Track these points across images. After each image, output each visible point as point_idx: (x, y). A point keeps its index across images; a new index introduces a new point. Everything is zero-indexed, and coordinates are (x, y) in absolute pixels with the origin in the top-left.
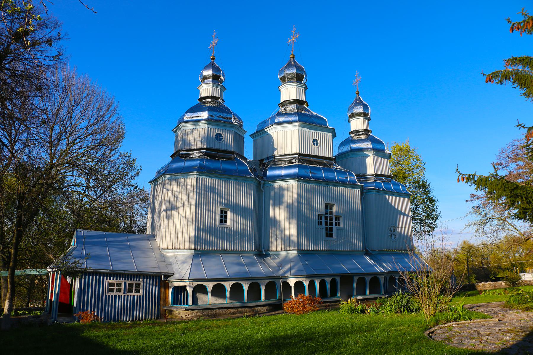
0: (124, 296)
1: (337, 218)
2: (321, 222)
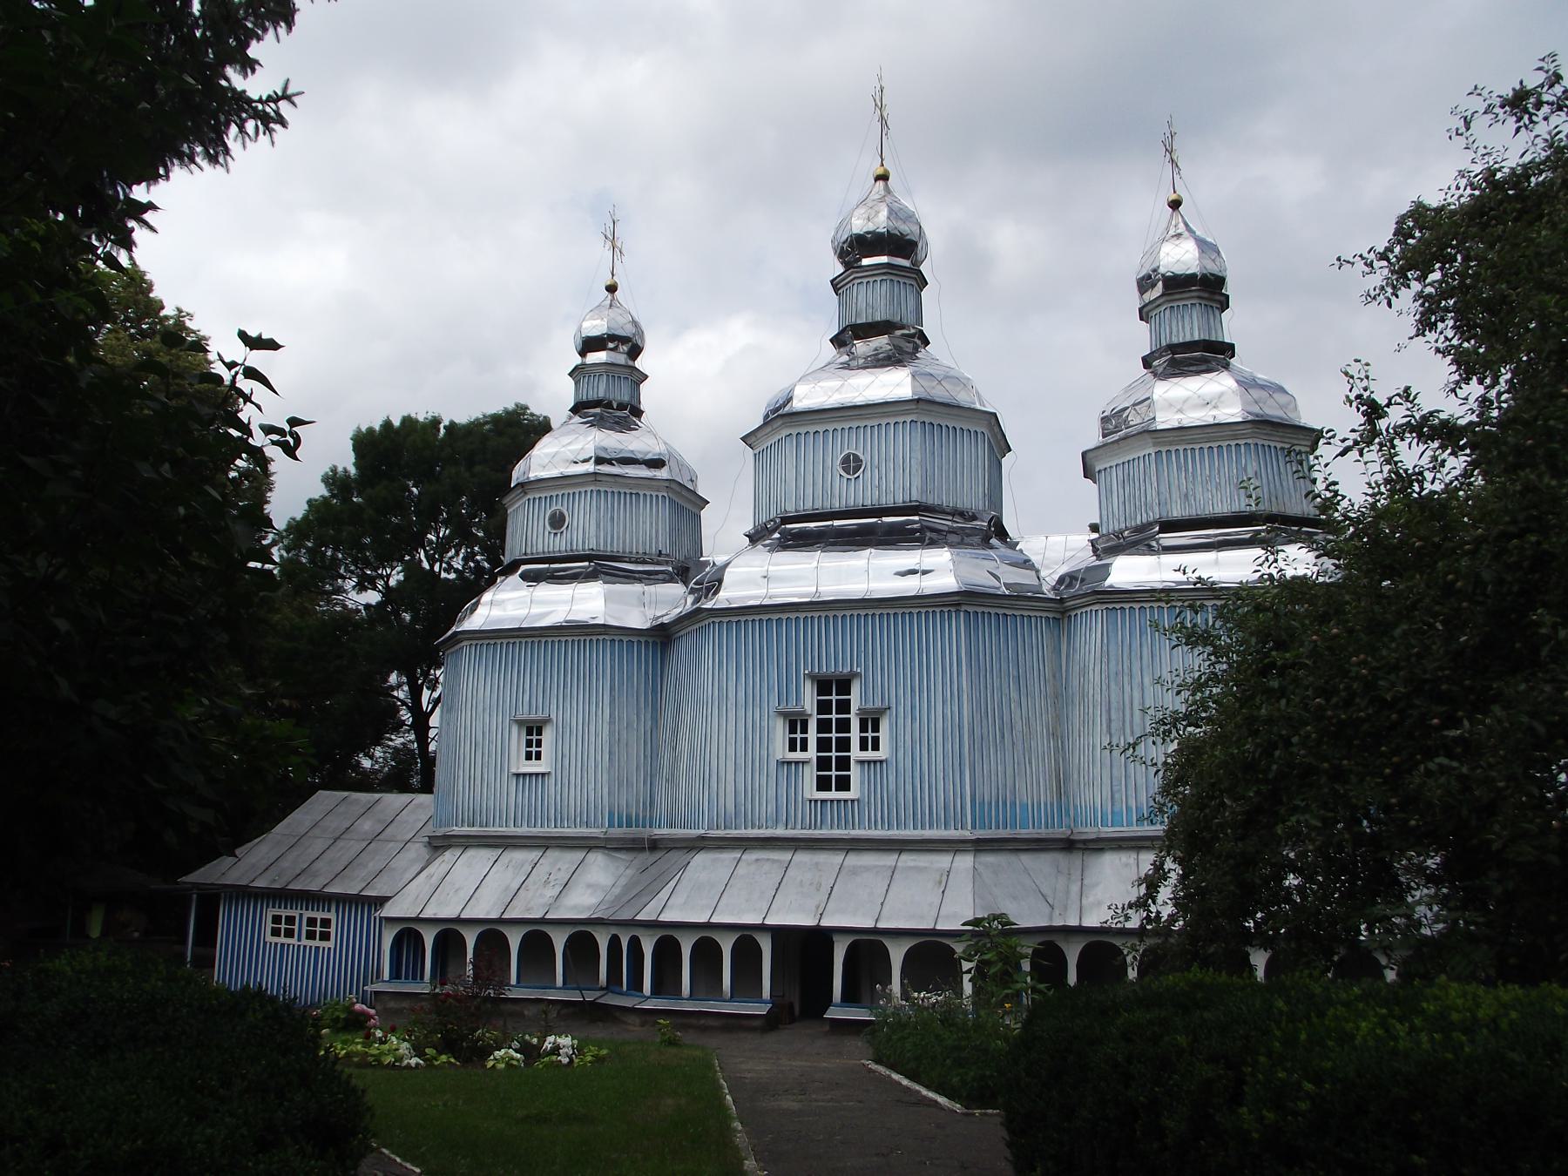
1: (871, 722)
2: (804, 742)
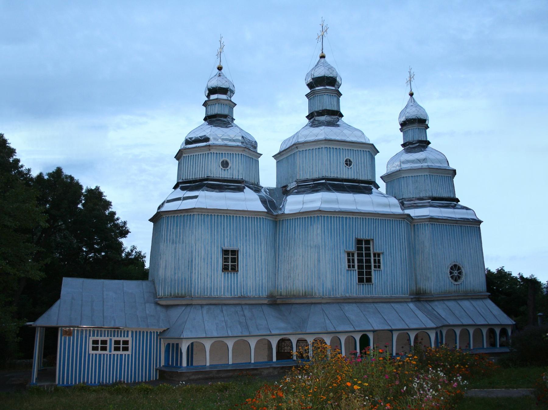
0: (110, 355)
